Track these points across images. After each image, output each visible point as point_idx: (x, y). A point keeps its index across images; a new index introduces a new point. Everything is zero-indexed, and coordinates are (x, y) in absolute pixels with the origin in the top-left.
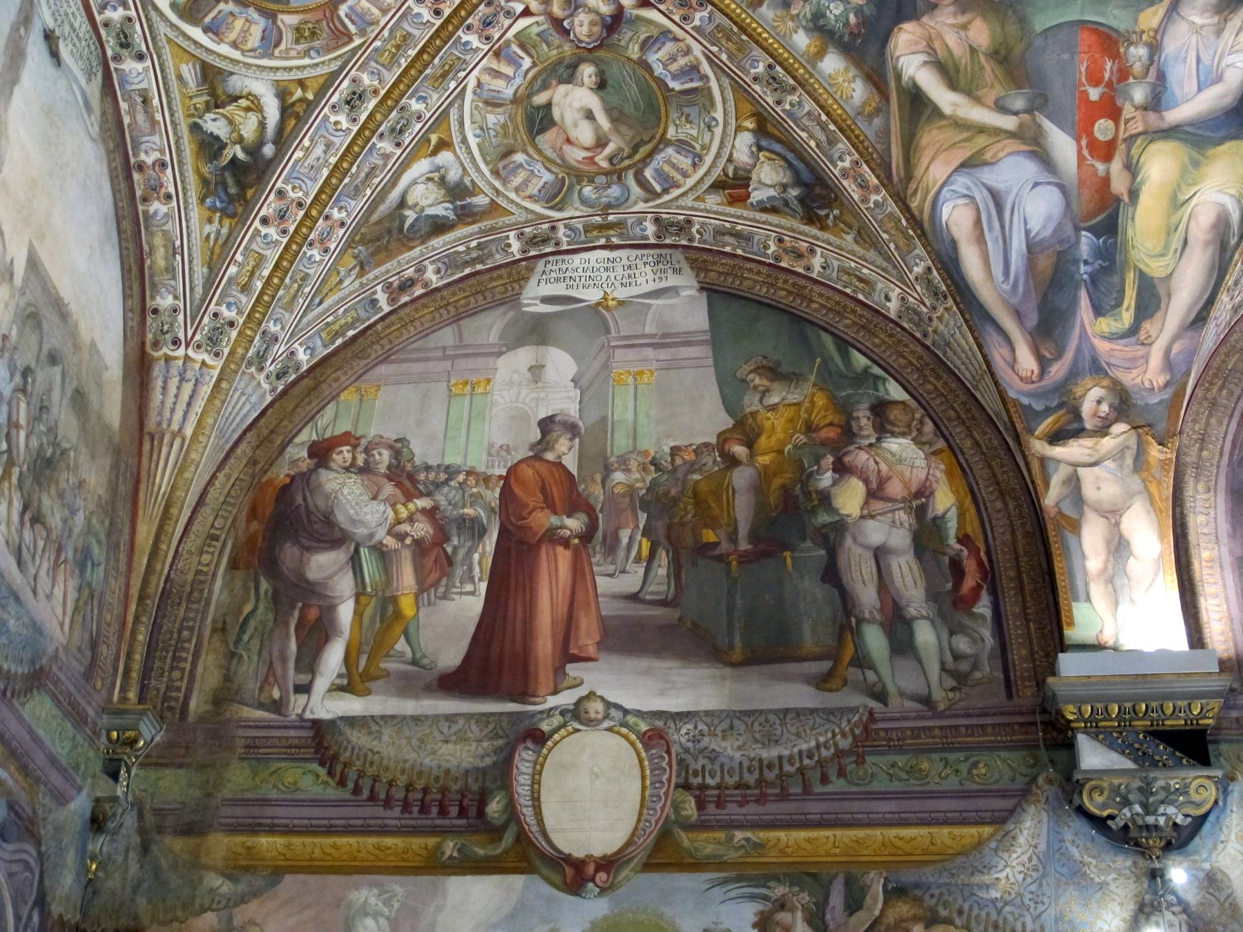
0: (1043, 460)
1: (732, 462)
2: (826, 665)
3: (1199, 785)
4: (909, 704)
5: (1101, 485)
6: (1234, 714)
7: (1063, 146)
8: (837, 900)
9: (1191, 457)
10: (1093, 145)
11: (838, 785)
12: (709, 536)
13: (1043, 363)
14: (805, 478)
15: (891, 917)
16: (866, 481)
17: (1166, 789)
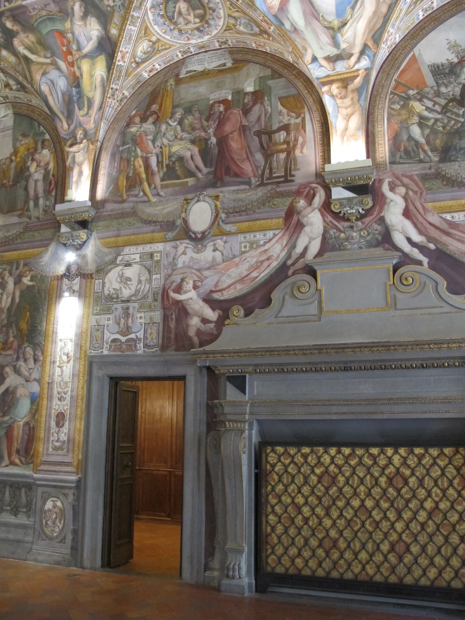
0: (68, 152)
1: (12, 161)
2: (21, 212)
3: (83, 234)
4: (35, 220)
5: (79, 157)
6: (98, 215)
7: (62, 65)
8: (14, 267)
9: (104, 146)
10: (69, 63)
11: (19, 241)
12: (5, 182)
13: (69, 125)
14: (25, 162)
15: (24, 270)
16: (37, 162)
17: (76, 235)
